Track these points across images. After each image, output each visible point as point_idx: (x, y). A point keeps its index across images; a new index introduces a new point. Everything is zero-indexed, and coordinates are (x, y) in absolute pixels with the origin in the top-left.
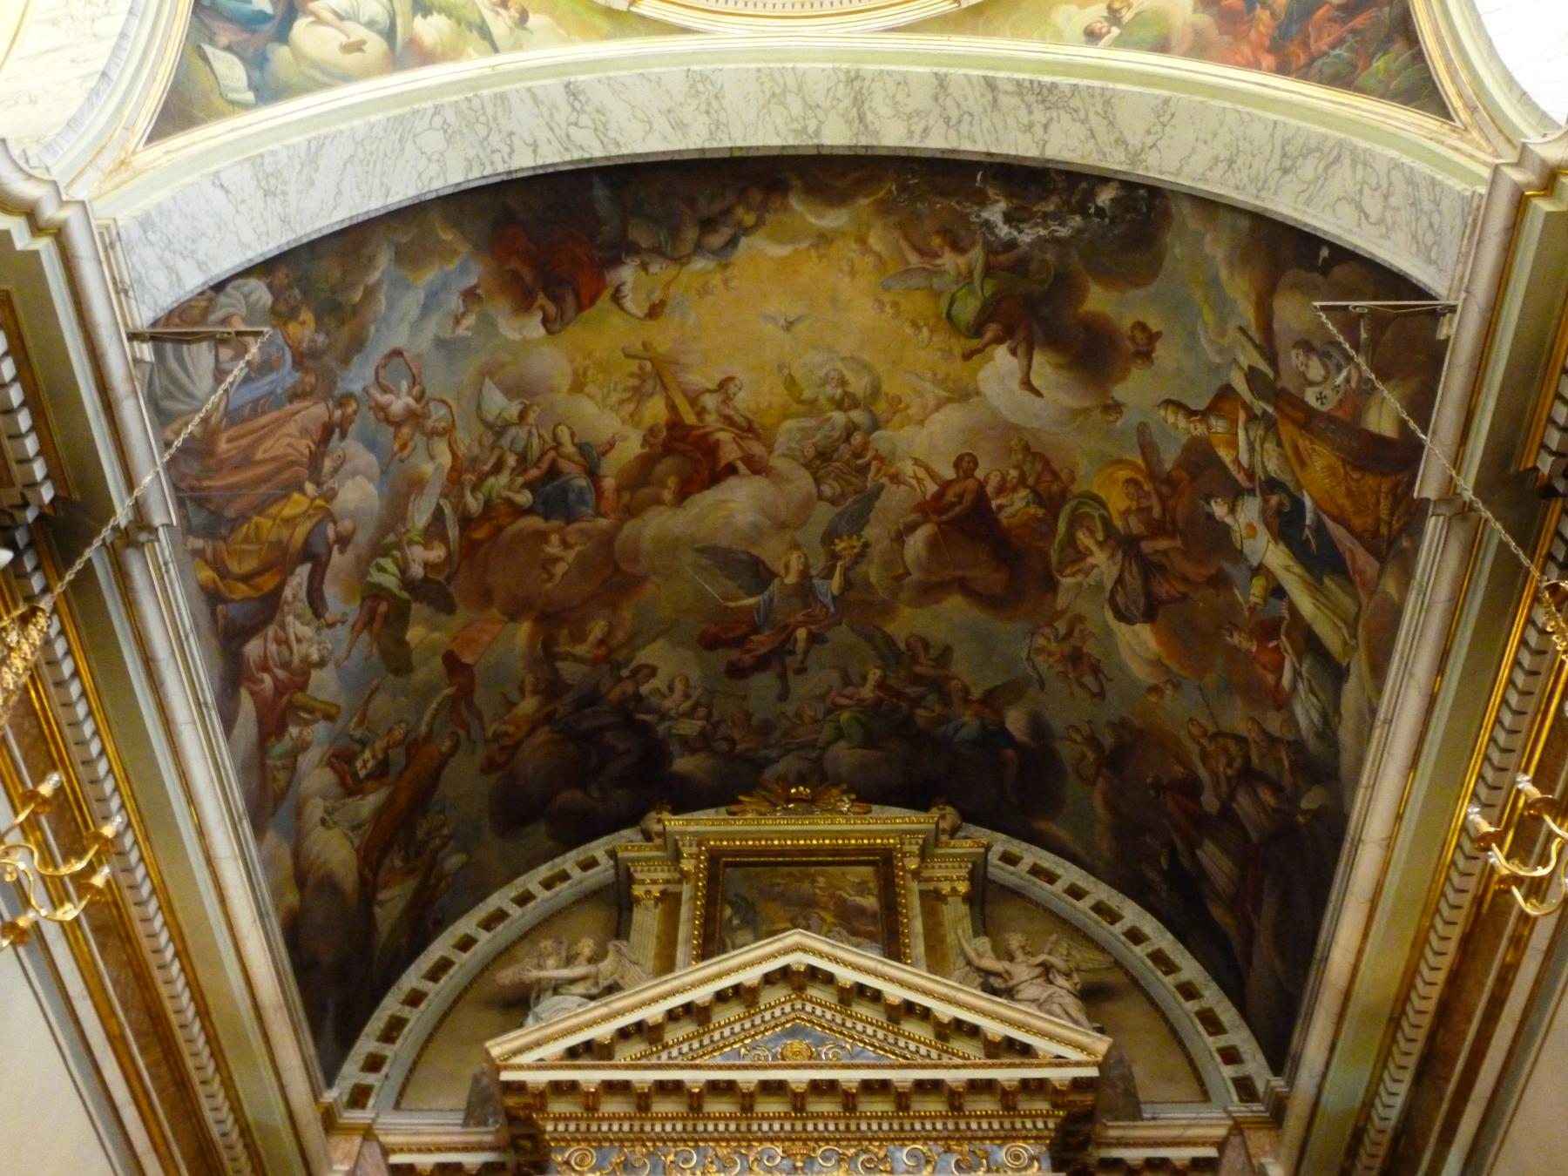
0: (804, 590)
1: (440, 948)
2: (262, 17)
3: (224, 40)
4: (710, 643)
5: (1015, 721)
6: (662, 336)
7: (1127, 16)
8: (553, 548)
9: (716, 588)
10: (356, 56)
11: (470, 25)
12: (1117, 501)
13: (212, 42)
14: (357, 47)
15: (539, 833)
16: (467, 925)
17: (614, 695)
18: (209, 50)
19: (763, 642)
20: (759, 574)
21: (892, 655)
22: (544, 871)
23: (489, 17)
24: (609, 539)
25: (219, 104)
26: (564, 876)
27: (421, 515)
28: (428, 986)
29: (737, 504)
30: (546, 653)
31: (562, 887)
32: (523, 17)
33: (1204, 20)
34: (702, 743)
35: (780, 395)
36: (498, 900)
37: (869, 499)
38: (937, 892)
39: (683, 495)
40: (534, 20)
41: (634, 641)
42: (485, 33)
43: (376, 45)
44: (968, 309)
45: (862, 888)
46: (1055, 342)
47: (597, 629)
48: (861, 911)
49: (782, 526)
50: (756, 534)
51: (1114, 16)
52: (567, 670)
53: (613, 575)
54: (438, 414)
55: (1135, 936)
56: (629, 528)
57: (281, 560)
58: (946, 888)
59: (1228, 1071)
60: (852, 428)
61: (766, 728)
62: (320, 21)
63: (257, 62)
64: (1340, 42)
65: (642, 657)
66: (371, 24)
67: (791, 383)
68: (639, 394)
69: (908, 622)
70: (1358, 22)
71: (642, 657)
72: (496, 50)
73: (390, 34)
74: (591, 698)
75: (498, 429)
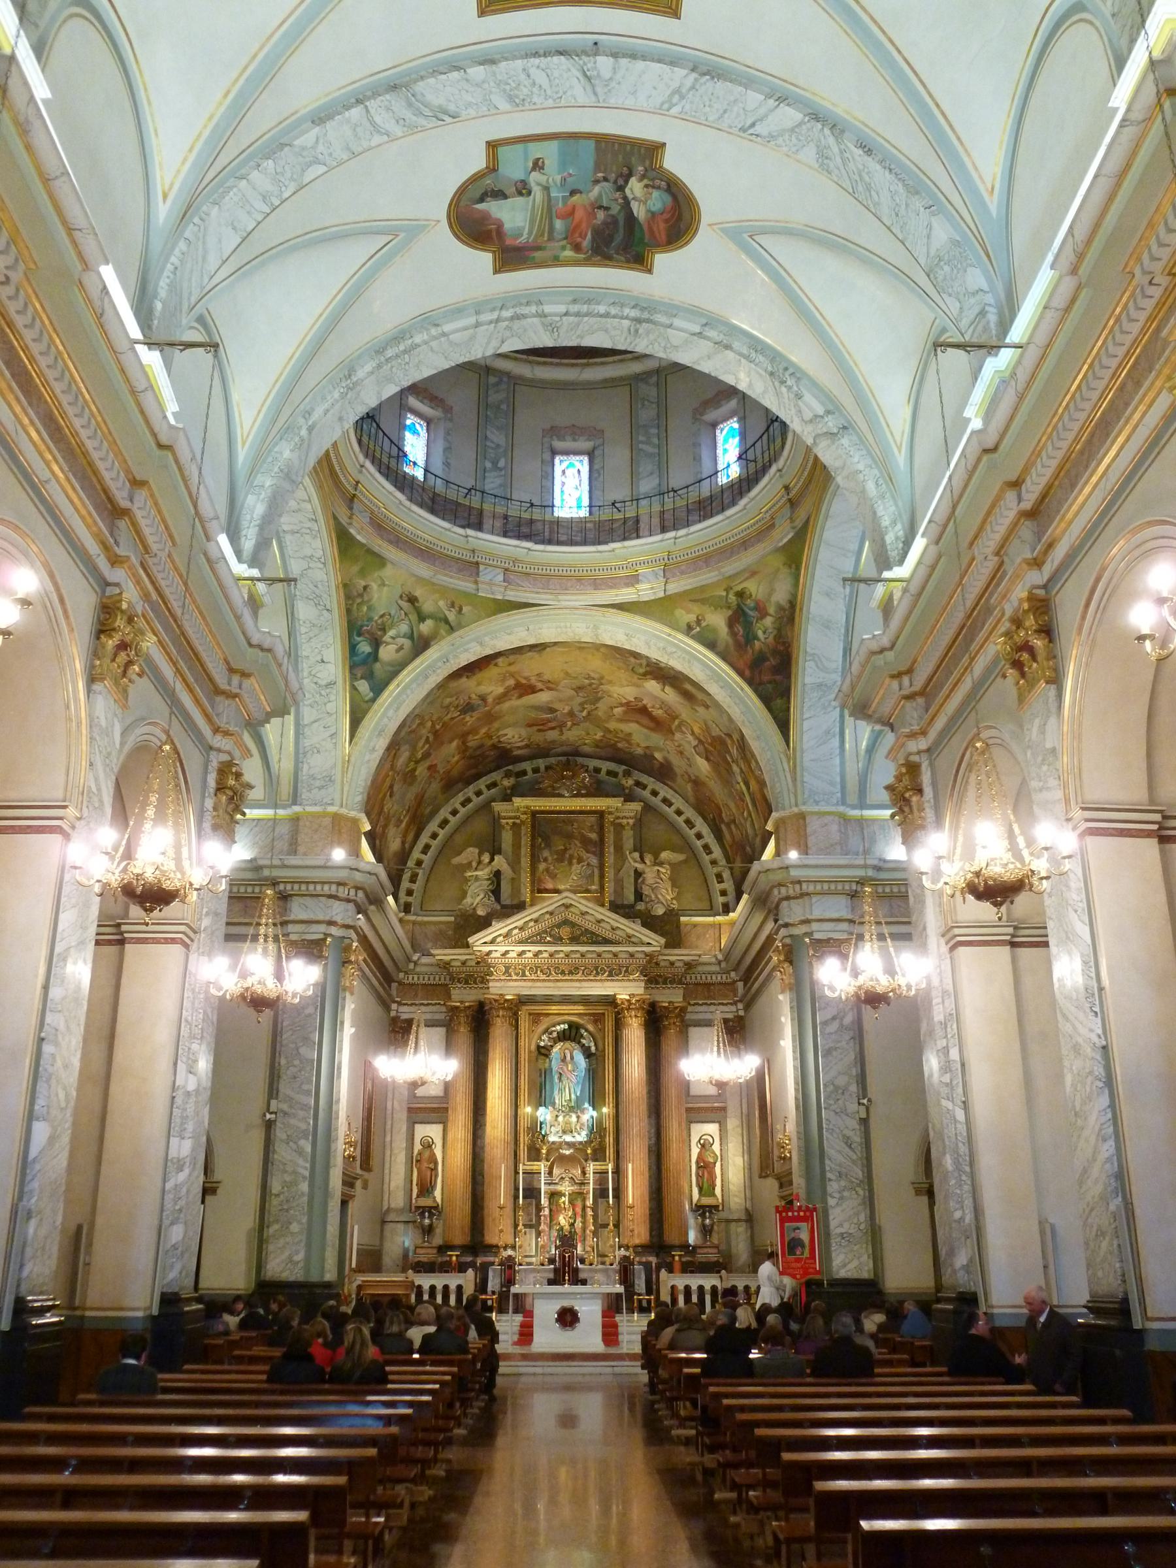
0: (571, 714)
1: (424, 839)
2: (369, 654)
3: (359, 675)
4: (530, 725)
5: (658, 755)
6: (512, 669)
7: (704, 624)
8: (468, 718)
9: (533, 714)
10: (401, 653)
11: (441, 620)
12: (697, 730)
13: (356, 679)
14: (401, 648)
15: (460, 785)
16: (433, 826)
17: (490, 743)
18: (355, 684)
19: (553, 724)
20: (552, 710)
21: (608, 731)
22: (461, 797)
23: (447, 613)
24: (489, 711)
25: (365, 706)
26: (468, 800)
27: (420, 744)
28: (423, 857)
29: (543, 697)
30: (464, 743)
31: (470, 805)
32: (461, 609)
33: (730, 641)
34: (527, 746)
35: (562, 675)
36: (444, 813)
37: (598, 699)
38: (620, 825)
39: (520, 696)
40: (465, 609)
41: (498, 730)
42: (447, 621)
43: (407, 643)
44: (642, 671)
45: (591, 829)
46: (673, 686)
47: (483, 731)
48: (590, 840)
49: (560, 701)
50: (551, 702)
51: (698, 622)
52: (469, 744)
53: (490, 718)
54: (426, 718)
55: (699, 836)
56: (497, 707)
57: (385, 795)
58: (624, 821)
59: (721, 899)
60: (590, 685)
61: (553, 742)
62: (388, 644)
63: (369, 676)
64: (770, 682)
65: (501, 733)
66: (404, 637)
67: (567, 674)
68: (503, 680)
69: (612, 725)
70: (778, 678)
71: (501, 733)
72: (452, 629)
73: (411, 637)
74: (481, 746)
75: (448, 707)
